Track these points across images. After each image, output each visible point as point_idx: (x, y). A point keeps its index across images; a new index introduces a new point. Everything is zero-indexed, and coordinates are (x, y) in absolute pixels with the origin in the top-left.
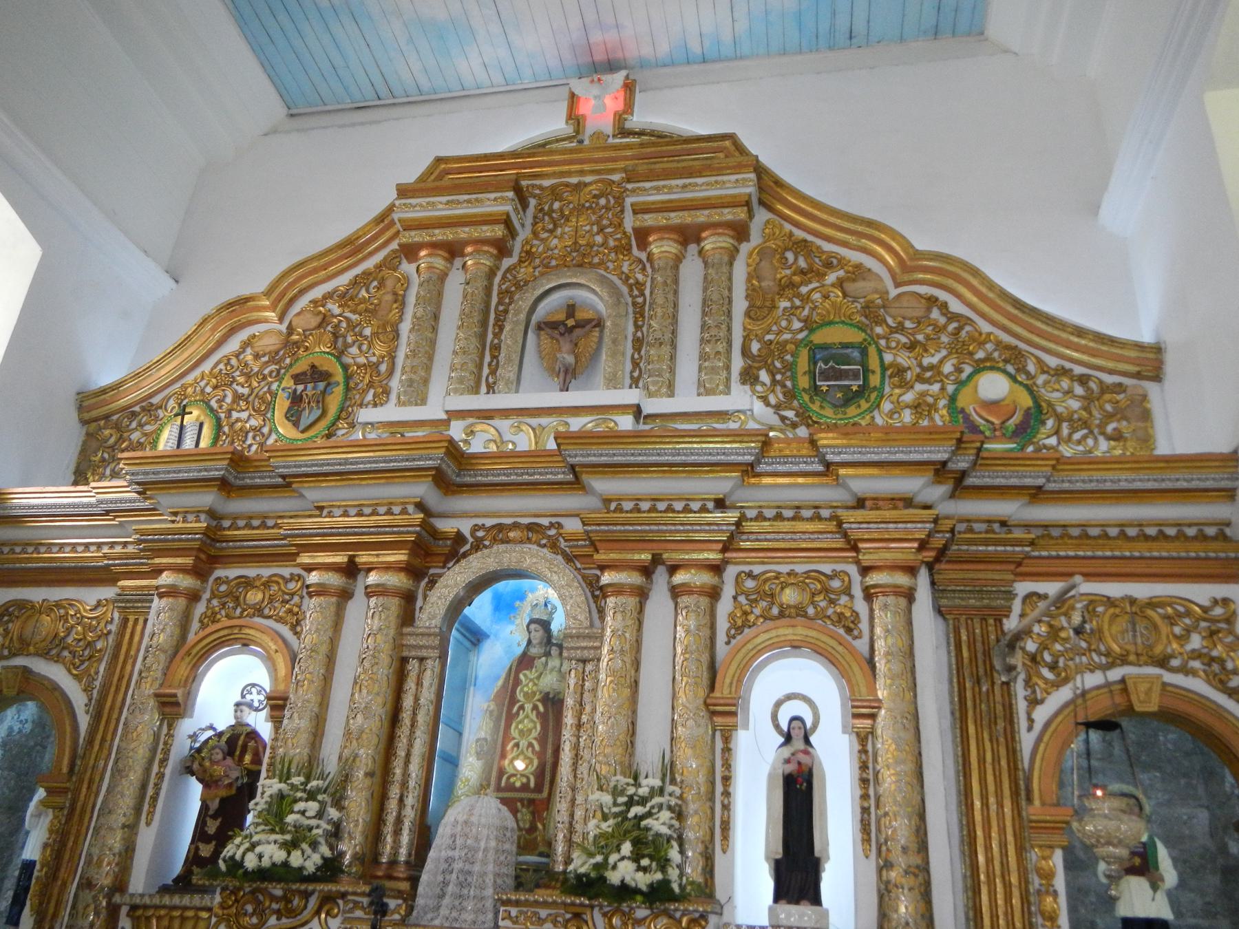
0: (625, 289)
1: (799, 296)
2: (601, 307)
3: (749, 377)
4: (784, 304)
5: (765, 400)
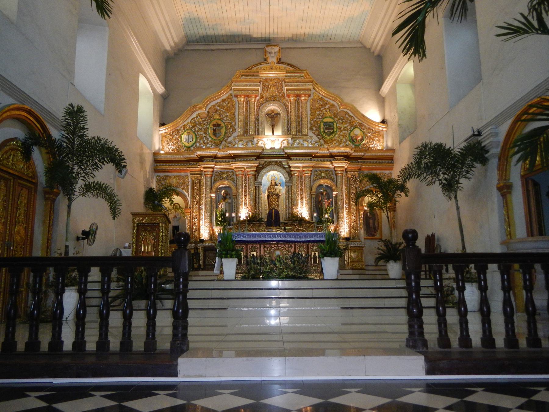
0: (284, 107)
1: (320, 110)
2: (279, 110)
3: (311, 129)
4: (318, 112)
5: (314, 133)
